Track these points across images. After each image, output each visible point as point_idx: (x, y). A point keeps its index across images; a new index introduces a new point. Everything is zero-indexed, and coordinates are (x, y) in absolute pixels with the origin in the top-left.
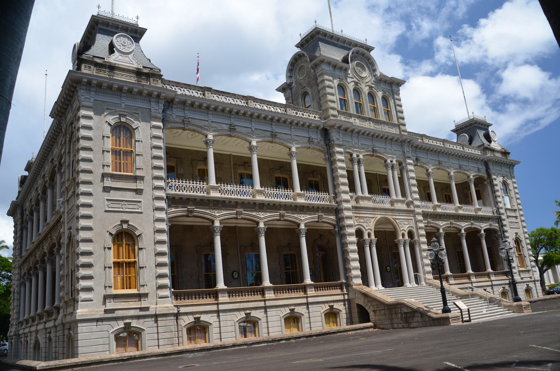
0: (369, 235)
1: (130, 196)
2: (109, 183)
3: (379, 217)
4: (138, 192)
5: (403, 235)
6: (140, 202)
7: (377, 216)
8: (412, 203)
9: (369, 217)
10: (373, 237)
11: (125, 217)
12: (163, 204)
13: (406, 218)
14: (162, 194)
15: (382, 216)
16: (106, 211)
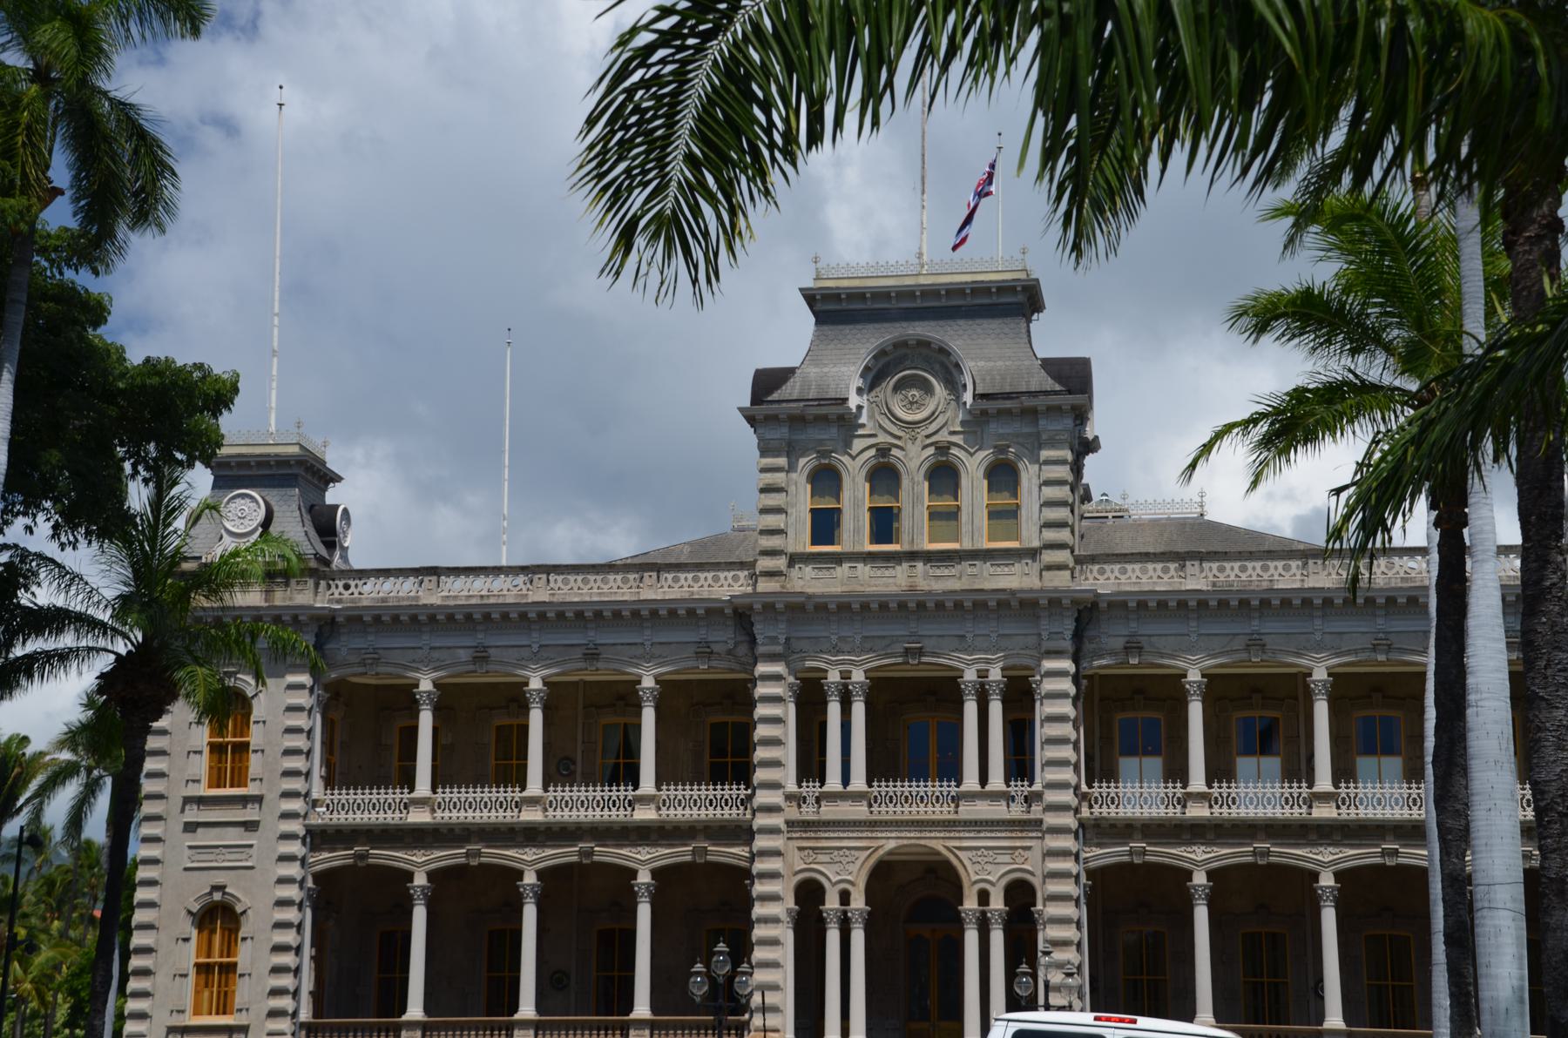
0: (845, 897)
1: (233, 836)
2: (193, 814)
3: (891, 844)
4: (250, 826)
5: (984, 897)
6: (251, 846)
7: (882, 842)
8: (1038, 796)
9: (849, 848)
10: (858, 902)
11: (219, 878)
12: (295, 848)
13: (1018, 843)
14: (296, 827)
15: (905, 842)
16: (186, 869)
